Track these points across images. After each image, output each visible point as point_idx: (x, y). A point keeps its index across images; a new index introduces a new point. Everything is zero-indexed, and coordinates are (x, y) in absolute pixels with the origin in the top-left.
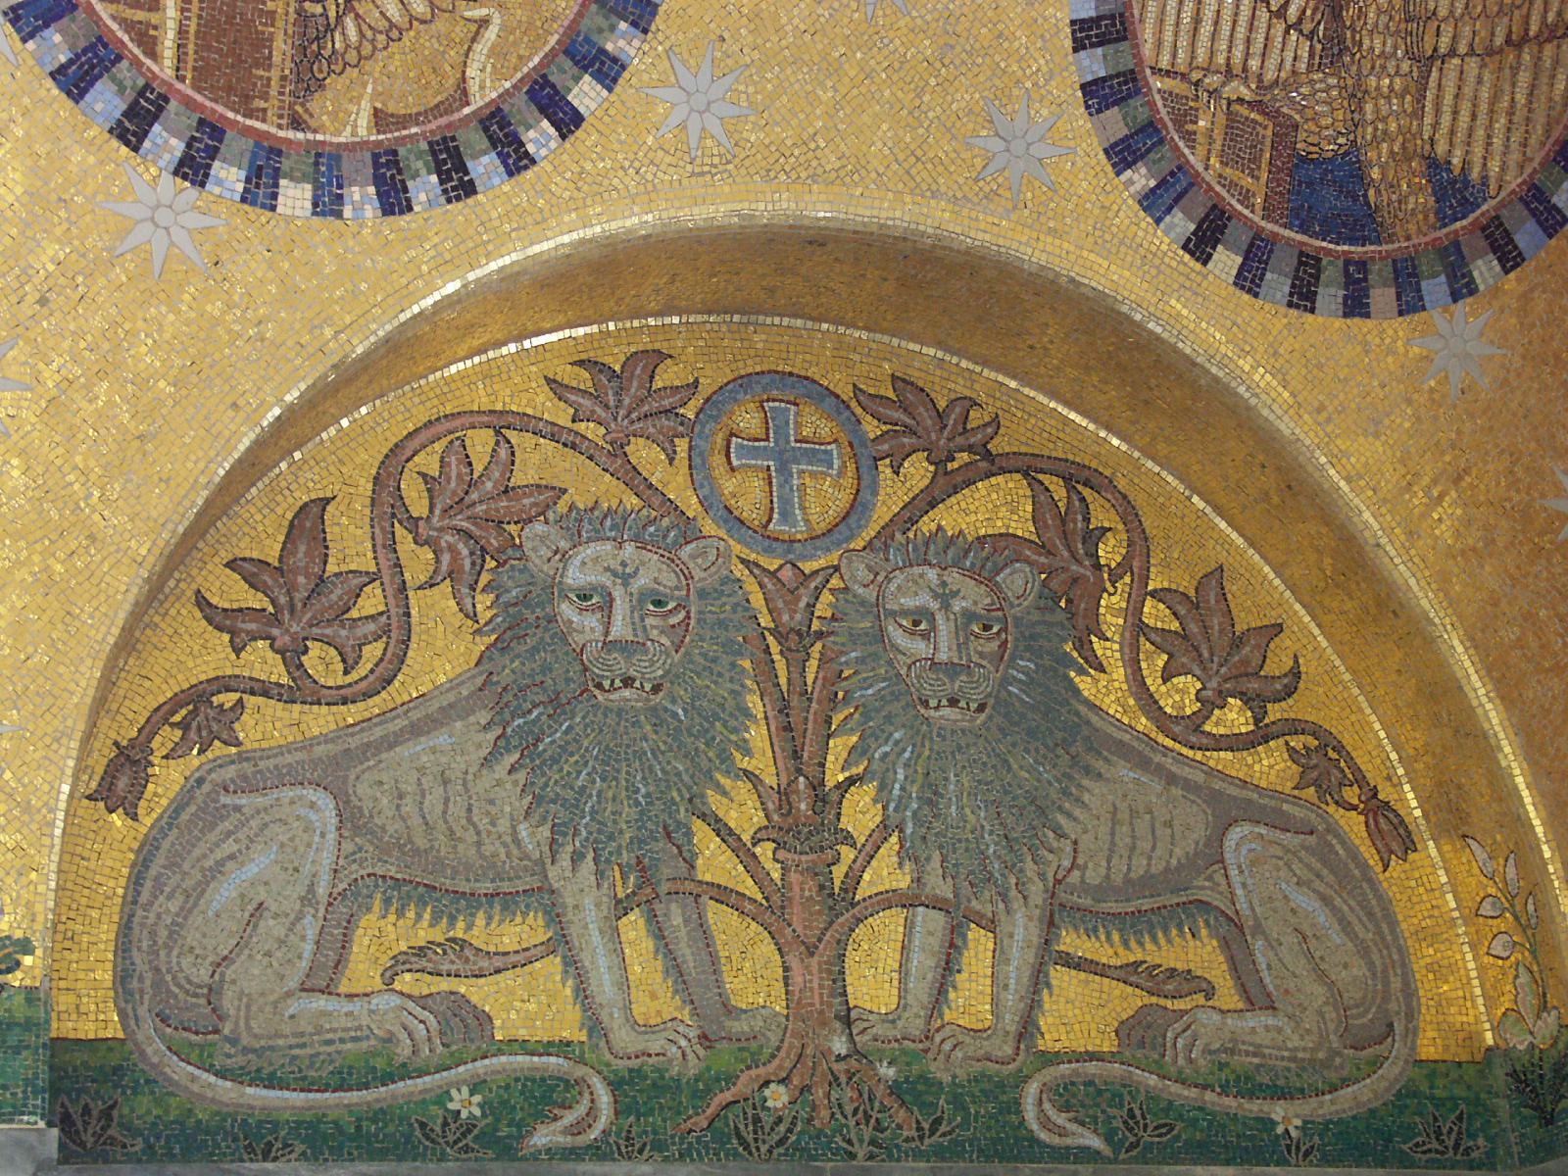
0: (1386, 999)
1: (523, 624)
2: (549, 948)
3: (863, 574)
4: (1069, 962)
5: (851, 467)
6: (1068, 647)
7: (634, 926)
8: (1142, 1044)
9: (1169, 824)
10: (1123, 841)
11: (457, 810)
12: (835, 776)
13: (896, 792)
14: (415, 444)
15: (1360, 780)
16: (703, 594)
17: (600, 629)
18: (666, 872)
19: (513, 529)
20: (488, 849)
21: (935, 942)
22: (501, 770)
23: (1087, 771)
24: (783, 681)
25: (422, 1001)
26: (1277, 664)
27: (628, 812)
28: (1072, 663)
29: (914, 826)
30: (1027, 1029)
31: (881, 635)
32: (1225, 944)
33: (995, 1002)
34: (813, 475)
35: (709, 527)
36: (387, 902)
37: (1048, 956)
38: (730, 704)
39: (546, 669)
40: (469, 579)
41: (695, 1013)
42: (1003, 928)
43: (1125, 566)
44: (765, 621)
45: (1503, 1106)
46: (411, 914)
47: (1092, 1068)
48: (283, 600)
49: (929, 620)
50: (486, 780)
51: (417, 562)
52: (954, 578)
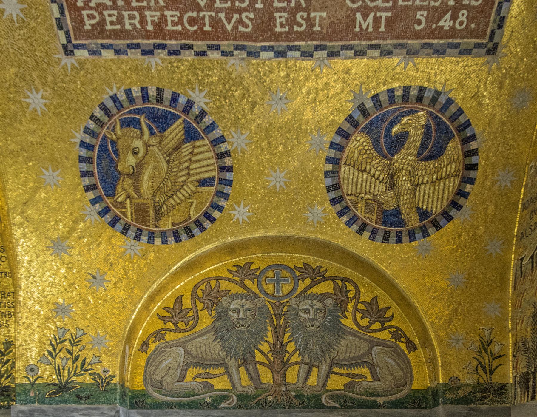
0: (406, 378)
2: (225, 373)
3: (294, 302)
4: (334, 373)
5: (293, 282)
6: (340, 314)
7: (242, 369)
8: (349, 388)
11: (208, 350)
12: (286, 340)
13: (299, 343)
15: (405, 336)
16: (259, 308)
18: (249, 359)
19: (220, 298)
20: (214, 356)
21: (305, 370)
22: (216, 343)
23: (342, 337)
24: (275, 324)
25: (200, 383)
27: (242, 349)
30: (324, 385)
31: (297, 314)
32: (370, 369)
35: (261, 295)
36: (194, 366)
37: (330, 372)
38: (264, 329)
39: (226, 324)
40: (210, 308)
41: (254, 384)
44: (272, 312)
46: (198, 368)
47: (338, 392)
49: (308, 310)
50: (213, 344)
51: (200, 306)
52: (315, 302)
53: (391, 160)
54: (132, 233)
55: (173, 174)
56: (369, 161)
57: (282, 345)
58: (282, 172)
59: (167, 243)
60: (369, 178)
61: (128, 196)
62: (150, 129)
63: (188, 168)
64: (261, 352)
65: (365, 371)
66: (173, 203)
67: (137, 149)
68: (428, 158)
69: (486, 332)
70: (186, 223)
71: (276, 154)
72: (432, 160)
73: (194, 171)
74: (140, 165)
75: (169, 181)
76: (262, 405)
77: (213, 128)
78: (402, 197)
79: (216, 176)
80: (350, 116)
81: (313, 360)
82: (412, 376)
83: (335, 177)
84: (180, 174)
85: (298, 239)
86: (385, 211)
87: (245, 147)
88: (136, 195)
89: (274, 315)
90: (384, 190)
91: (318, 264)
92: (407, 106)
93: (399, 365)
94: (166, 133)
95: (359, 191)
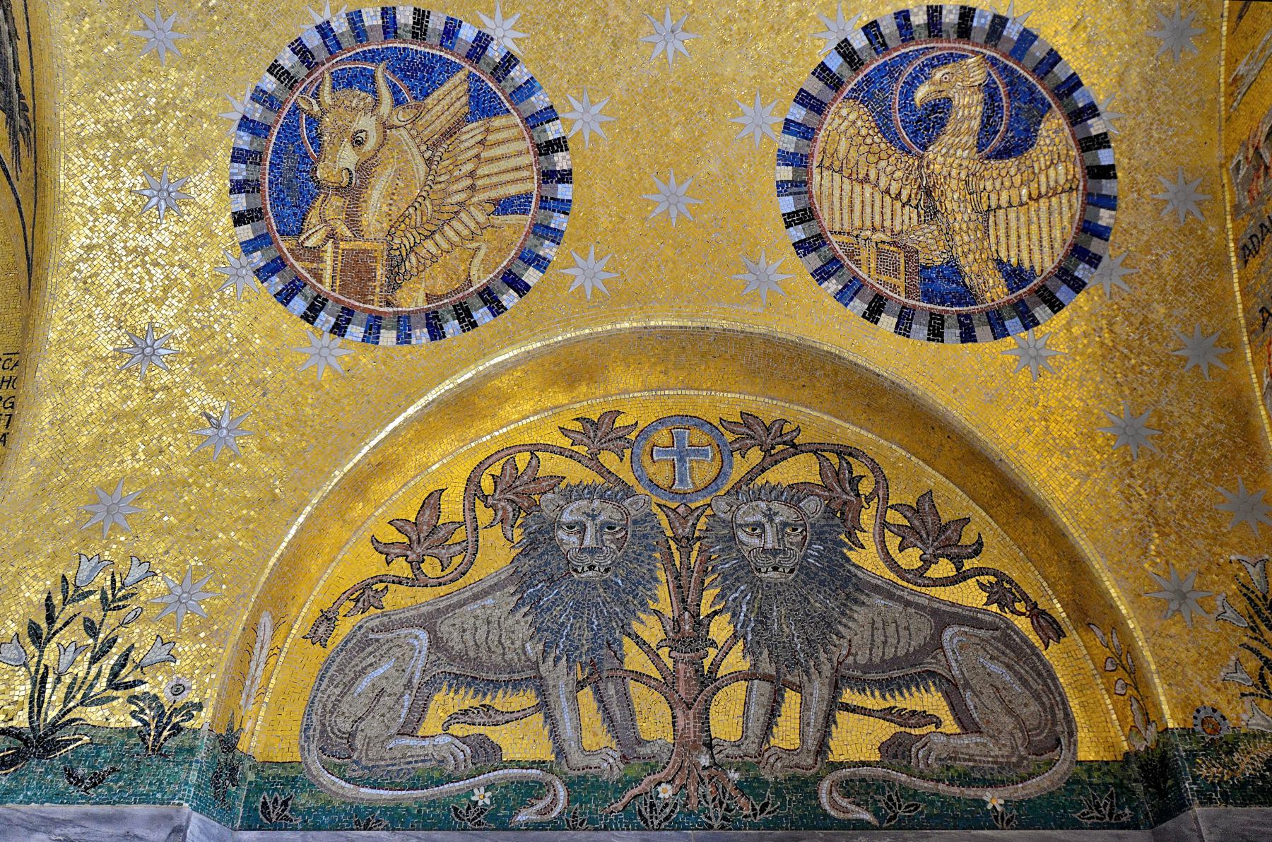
0: (1054, 723)
1: (539, 542)
2: (537, 708)
5: (718, 456)
6: (842, 537)
8: (895, 756)
9: (907, 628)
10: (879, 639)
11: (494, 637)
12: (705, 610)
13: (742, 618)
14: (490, 461)
15: (1026, 598)
16: (635, 522)
17: (578, 542)
18: (607, 666)
20: (508, 657)
21: (764, 700)
22: (519, 615)
23: (856, 601)
24: (677, 563)
26: (968, 538)
28: (845, 544)
29: (756, 635)
30: (822, 748)
31: (733, 537)
32: (947, 695)
33: (802, 734)
34: (698, 462)
36: (450, 686)
41: (619, 743)
42: (807, 690)
43: (875, 493)
44: (669, 533)
45: (1139, 788)
46: (462, 692)
47: (864, 771)
48: (414, 538)
52: (775, 506)
53: (922, 157)
54: (326, 319)
55: (439, 186)
56: (872, 159)
57: (698, 623)
58: (682, 183)
59: (409, 343)
60: (878, 196)
61: (332, 235)
62: (395, 91)
63: (471, 174)
64: (641, 643)
65: (931, 701)
66: (434, 250)
67: (363, 135)
68: (1004, 153)
69: (1251, 569)
70: (461, 295)
71: (667, 144)
72: (1010, 156)
73: (487, 181)
74: (365, 169)
75: (427, 202)
76: (642, 815)
77: (529, 90)
78: (957, 238)
79: (535, 193)
80: (823, 66)
81: (784, 669)
82: (1068, 718)
83: (800, 193)
84: (455, 187)
85: (724, 336)
86: (925, 268)
87: (599, 130)
88: (349, 233)
89: (674, 539)
90: (914, 221)
91: (777, 414)
92: (940, 45)
93: (1025, 683)
94: (429, 101)
95: (857, 223)
